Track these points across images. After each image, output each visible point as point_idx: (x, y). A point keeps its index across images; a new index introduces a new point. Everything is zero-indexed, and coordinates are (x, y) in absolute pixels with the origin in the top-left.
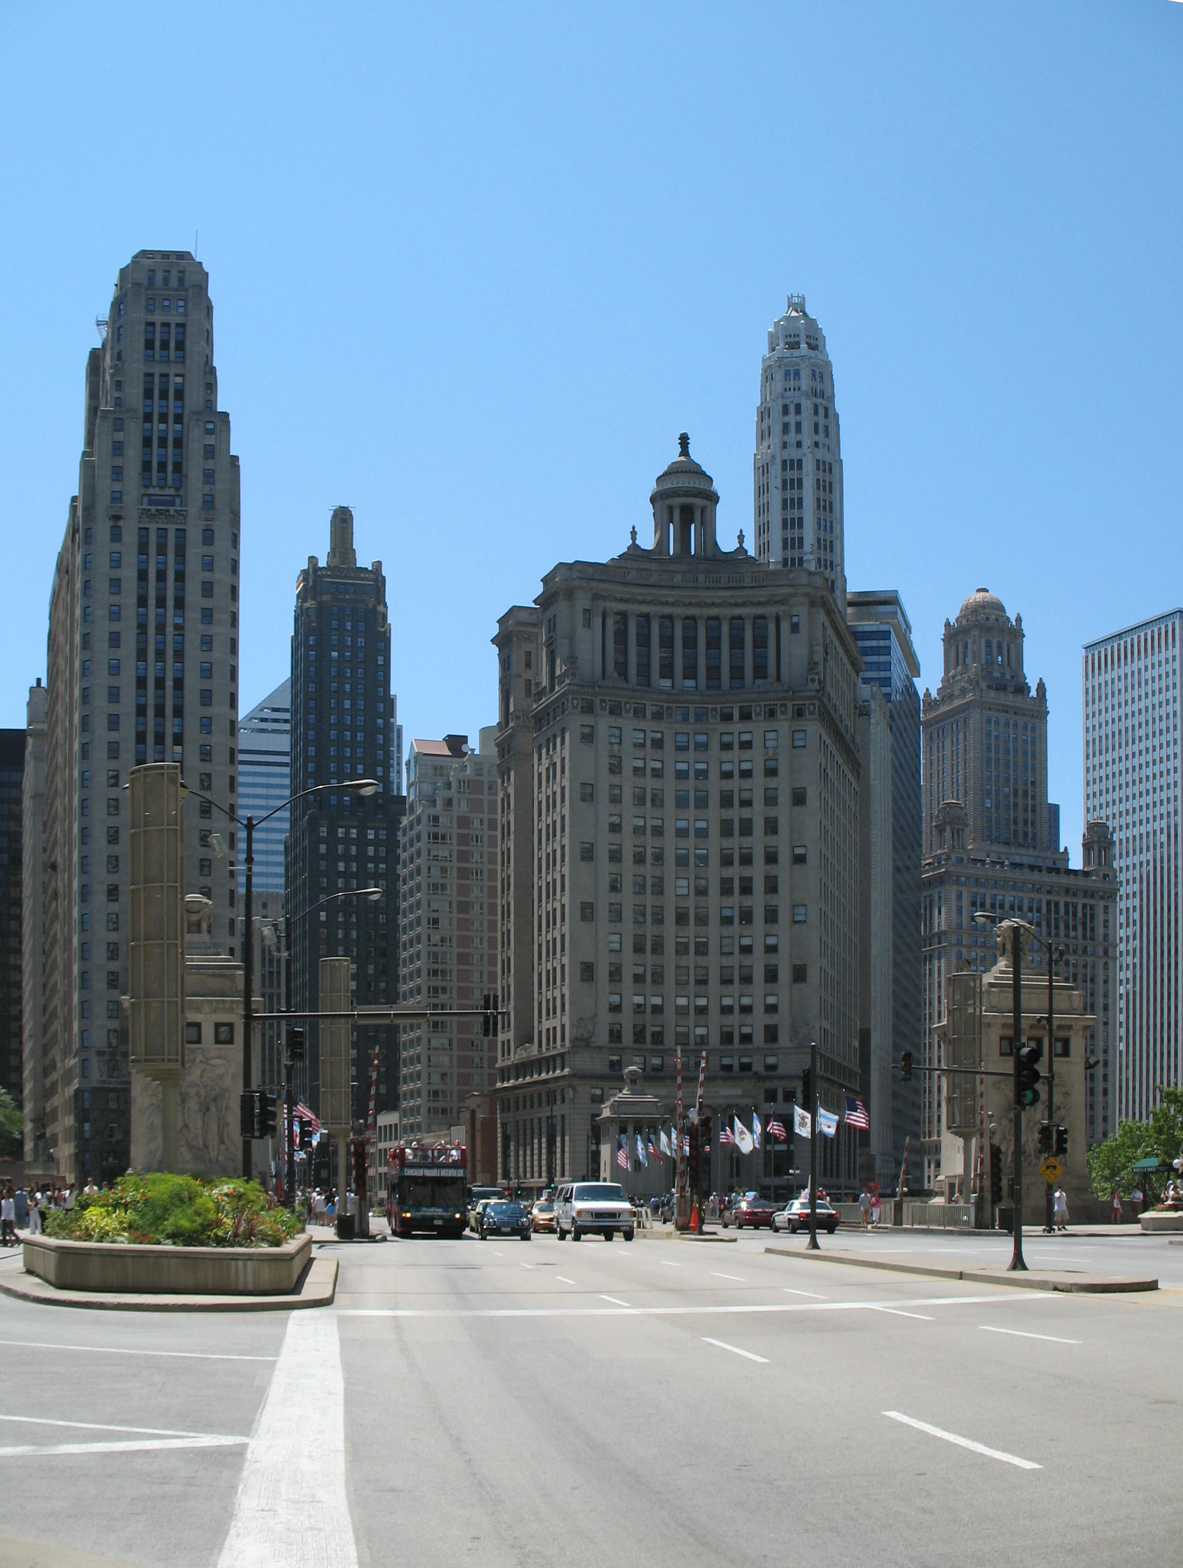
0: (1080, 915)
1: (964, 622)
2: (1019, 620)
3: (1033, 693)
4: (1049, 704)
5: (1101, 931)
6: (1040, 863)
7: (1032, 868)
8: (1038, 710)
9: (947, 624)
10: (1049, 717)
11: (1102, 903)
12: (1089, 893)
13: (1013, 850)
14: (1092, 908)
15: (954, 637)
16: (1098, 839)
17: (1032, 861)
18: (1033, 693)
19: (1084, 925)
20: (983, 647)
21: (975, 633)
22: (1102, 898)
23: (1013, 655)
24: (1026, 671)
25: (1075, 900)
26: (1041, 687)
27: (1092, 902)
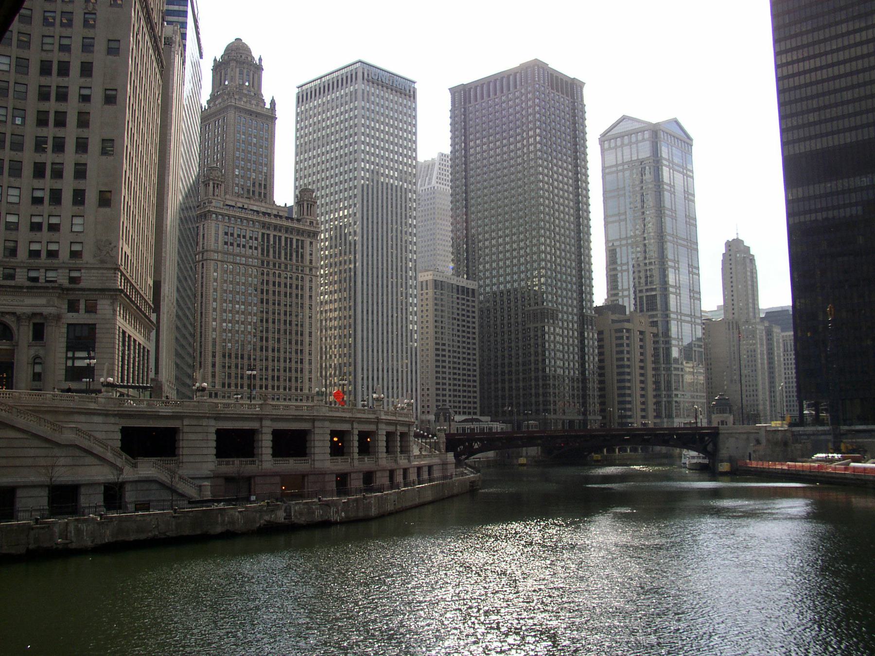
0: (294, 246)
1: (226, 57)
2: (260, 59)
3: (268, 106)
4: (277, 113)
5: (308, 257)
6: (269, 211)
7: (264, 214)
8: (270, 117)
9: (215, 60)
10: (277, 121)
11: (307, 241)
12: (299, 232)
13: (252, 202)
14: (302, 241)
15: (219, 68)
16: (305, 197)
17: (263, 210)
18: (268, 106)
19: (297, 252)
20: (237, 74)
21: (233, 64)
22: (309, 236)
23: (256, 80)
24: (263, 92)
25: (291, 236)
26: (273, 103)
27: (302, 238)
